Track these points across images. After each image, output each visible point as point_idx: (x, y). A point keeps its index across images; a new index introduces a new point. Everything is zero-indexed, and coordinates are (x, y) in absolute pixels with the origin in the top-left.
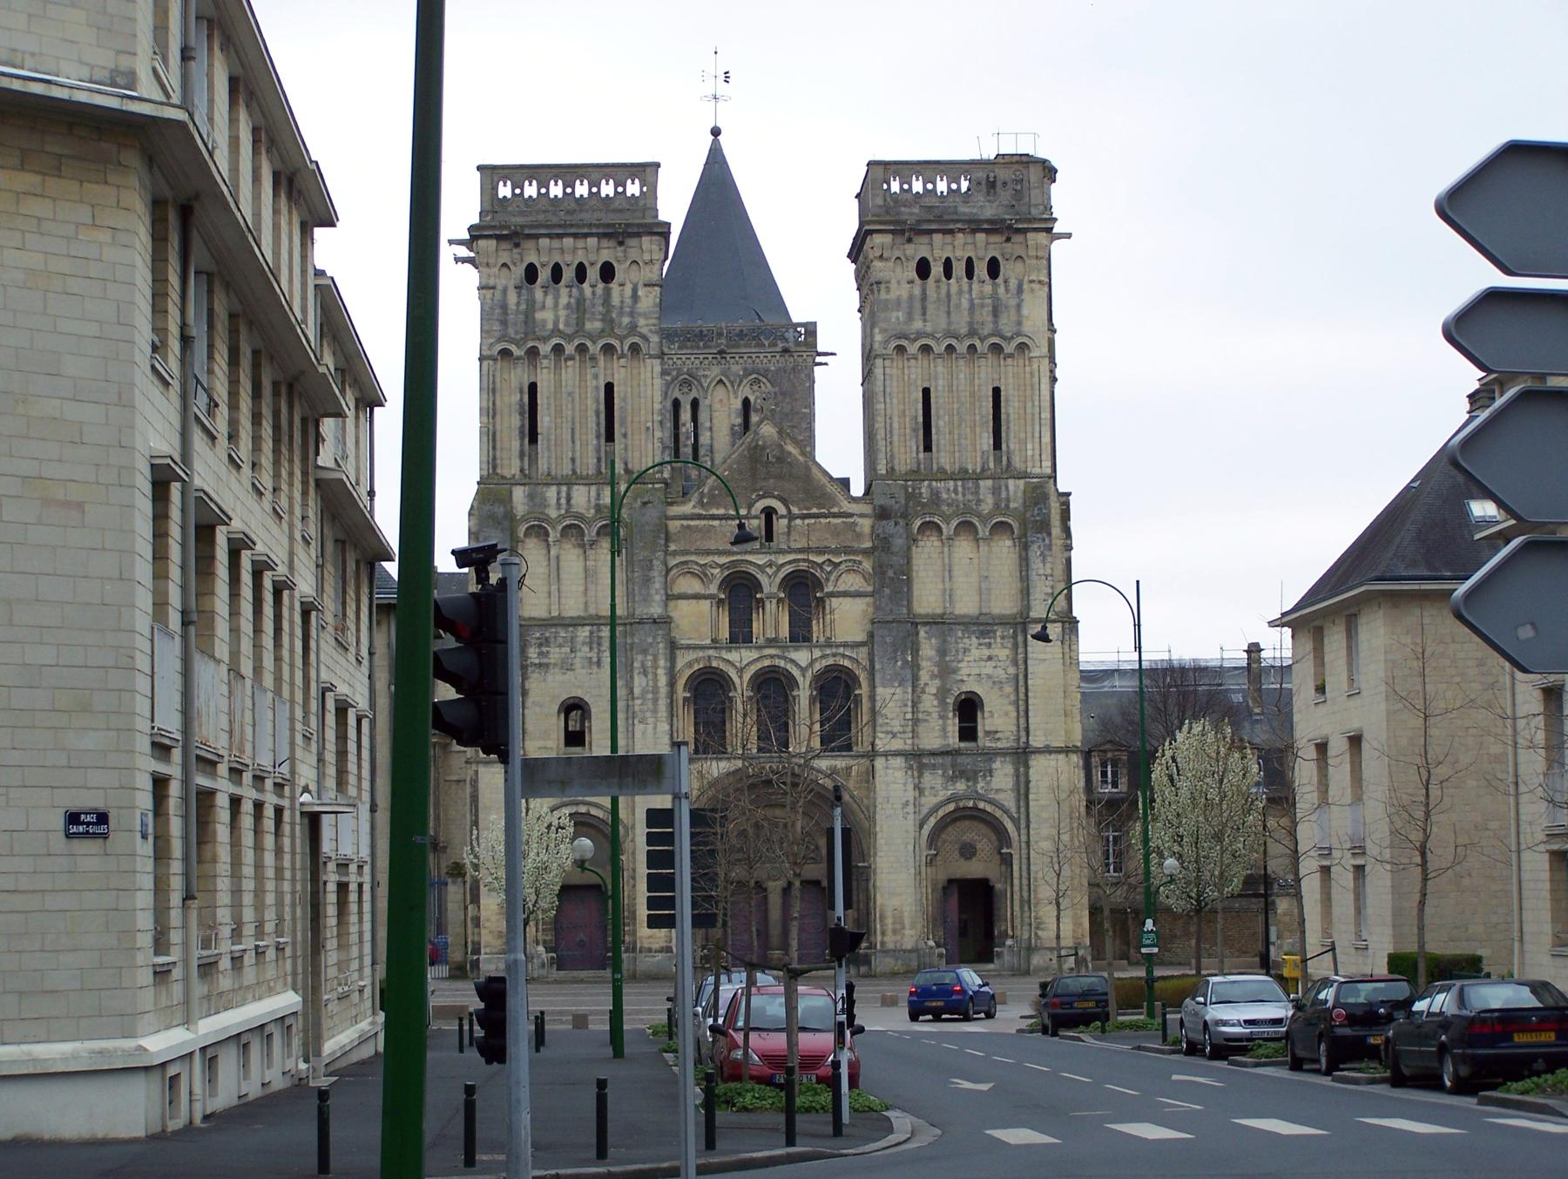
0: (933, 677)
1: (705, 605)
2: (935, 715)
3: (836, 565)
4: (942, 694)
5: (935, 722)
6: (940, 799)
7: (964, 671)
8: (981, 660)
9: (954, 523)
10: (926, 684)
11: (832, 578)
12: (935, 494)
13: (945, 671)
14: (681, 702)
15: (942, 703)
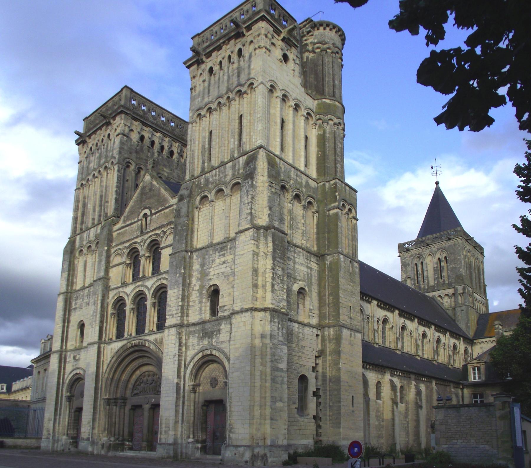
0: (198, 280)
1: (121, 266)
2: (197, 302)
3: (165, 233)
4: (200, 291)
5: (197, 307)
6: (196, 351)
7: (212, 274)
8: (220, 264)
9: (214, 192)
10: (195, 285)
11: (164, 240)
12: (207, 180)
13: (204, 274)
14: (109, 316)
15: (201, 294)
